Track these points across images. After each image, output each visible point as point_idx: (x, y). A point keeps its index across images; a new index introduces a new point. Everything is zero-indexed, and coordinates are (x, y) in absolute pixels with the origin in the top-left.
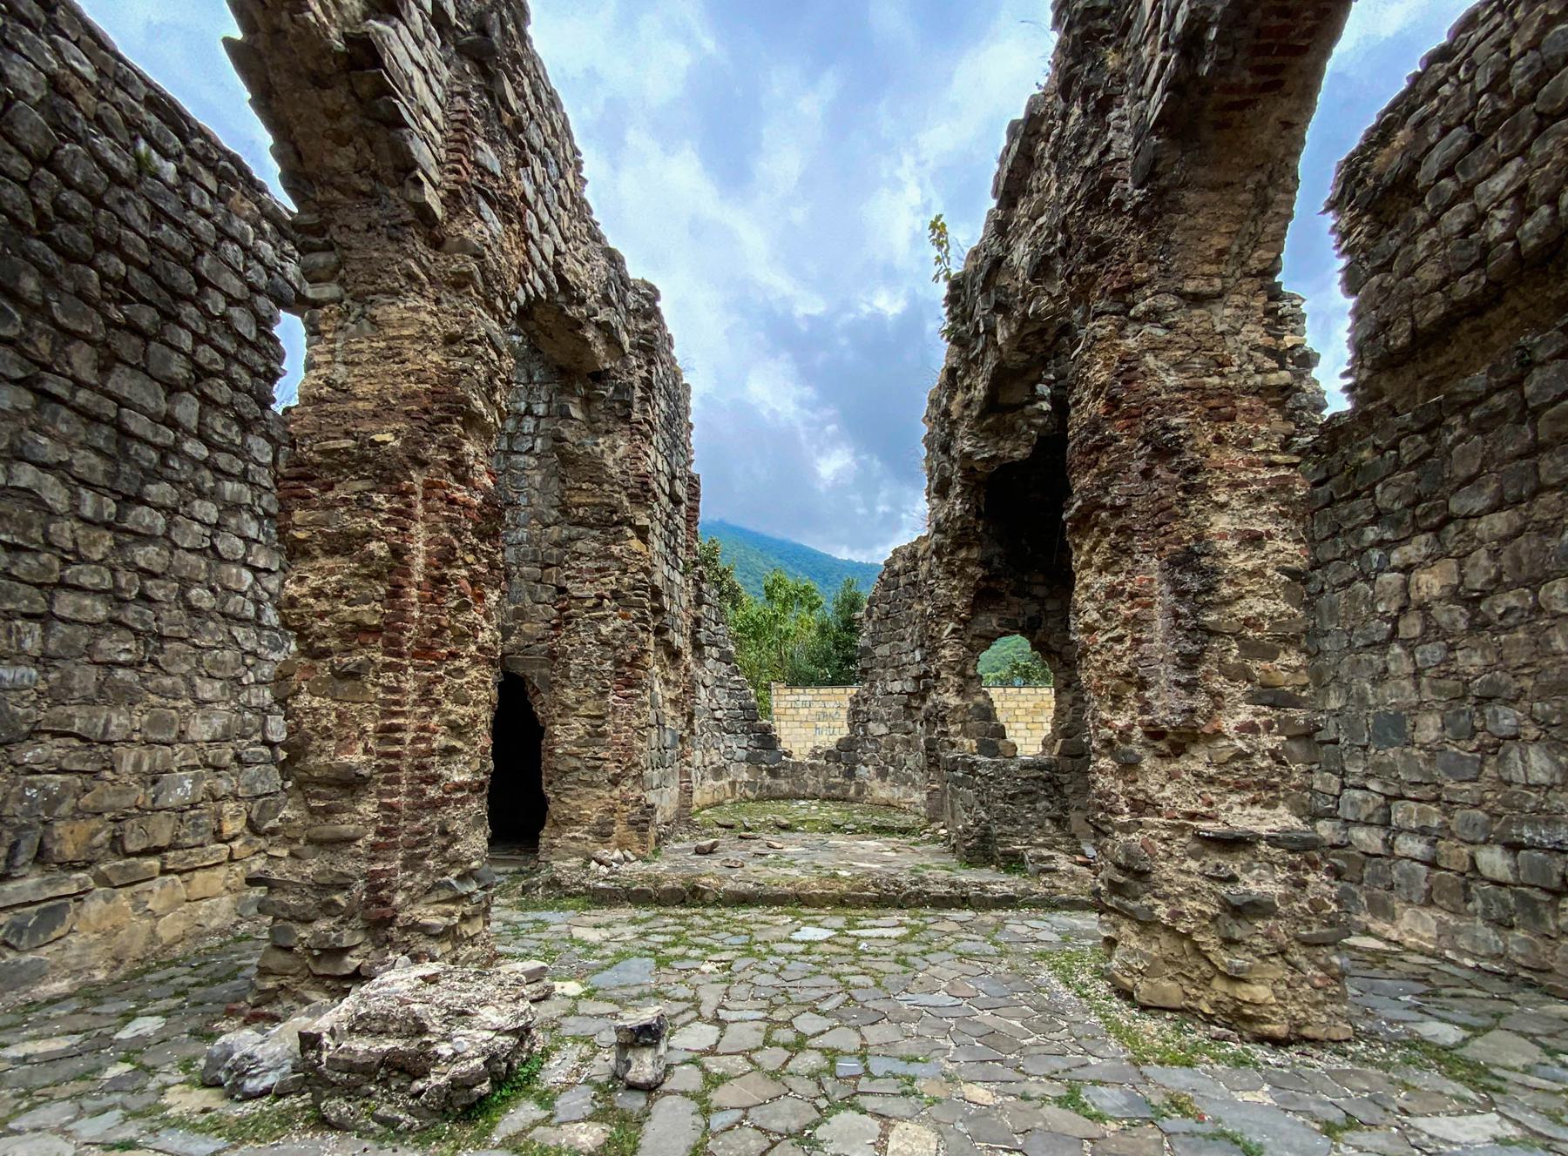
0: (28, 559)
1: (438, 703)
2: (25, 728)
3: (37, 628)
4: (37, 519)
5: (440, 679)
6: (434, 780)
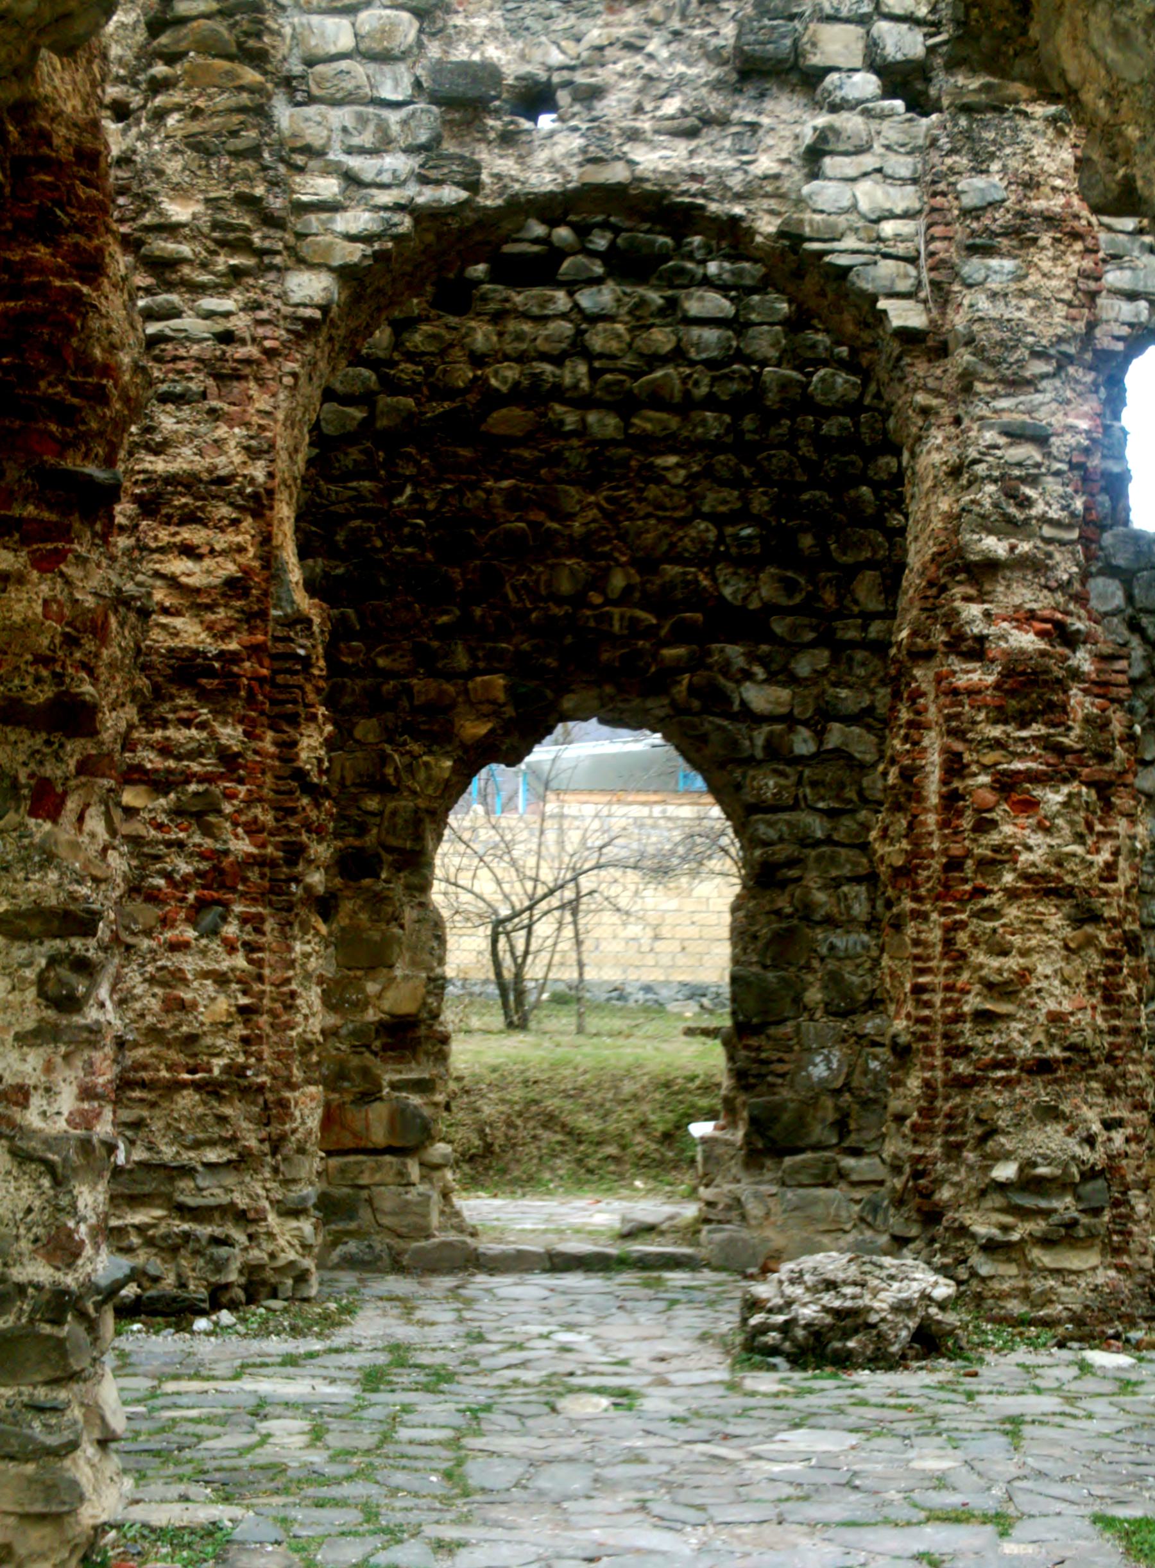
0: (847, 822)
1: (963, 955)
2: (862, 997)
3: (862, 890)
4: (846, 775)
5: (962, 925)
6: (963, 1052)
